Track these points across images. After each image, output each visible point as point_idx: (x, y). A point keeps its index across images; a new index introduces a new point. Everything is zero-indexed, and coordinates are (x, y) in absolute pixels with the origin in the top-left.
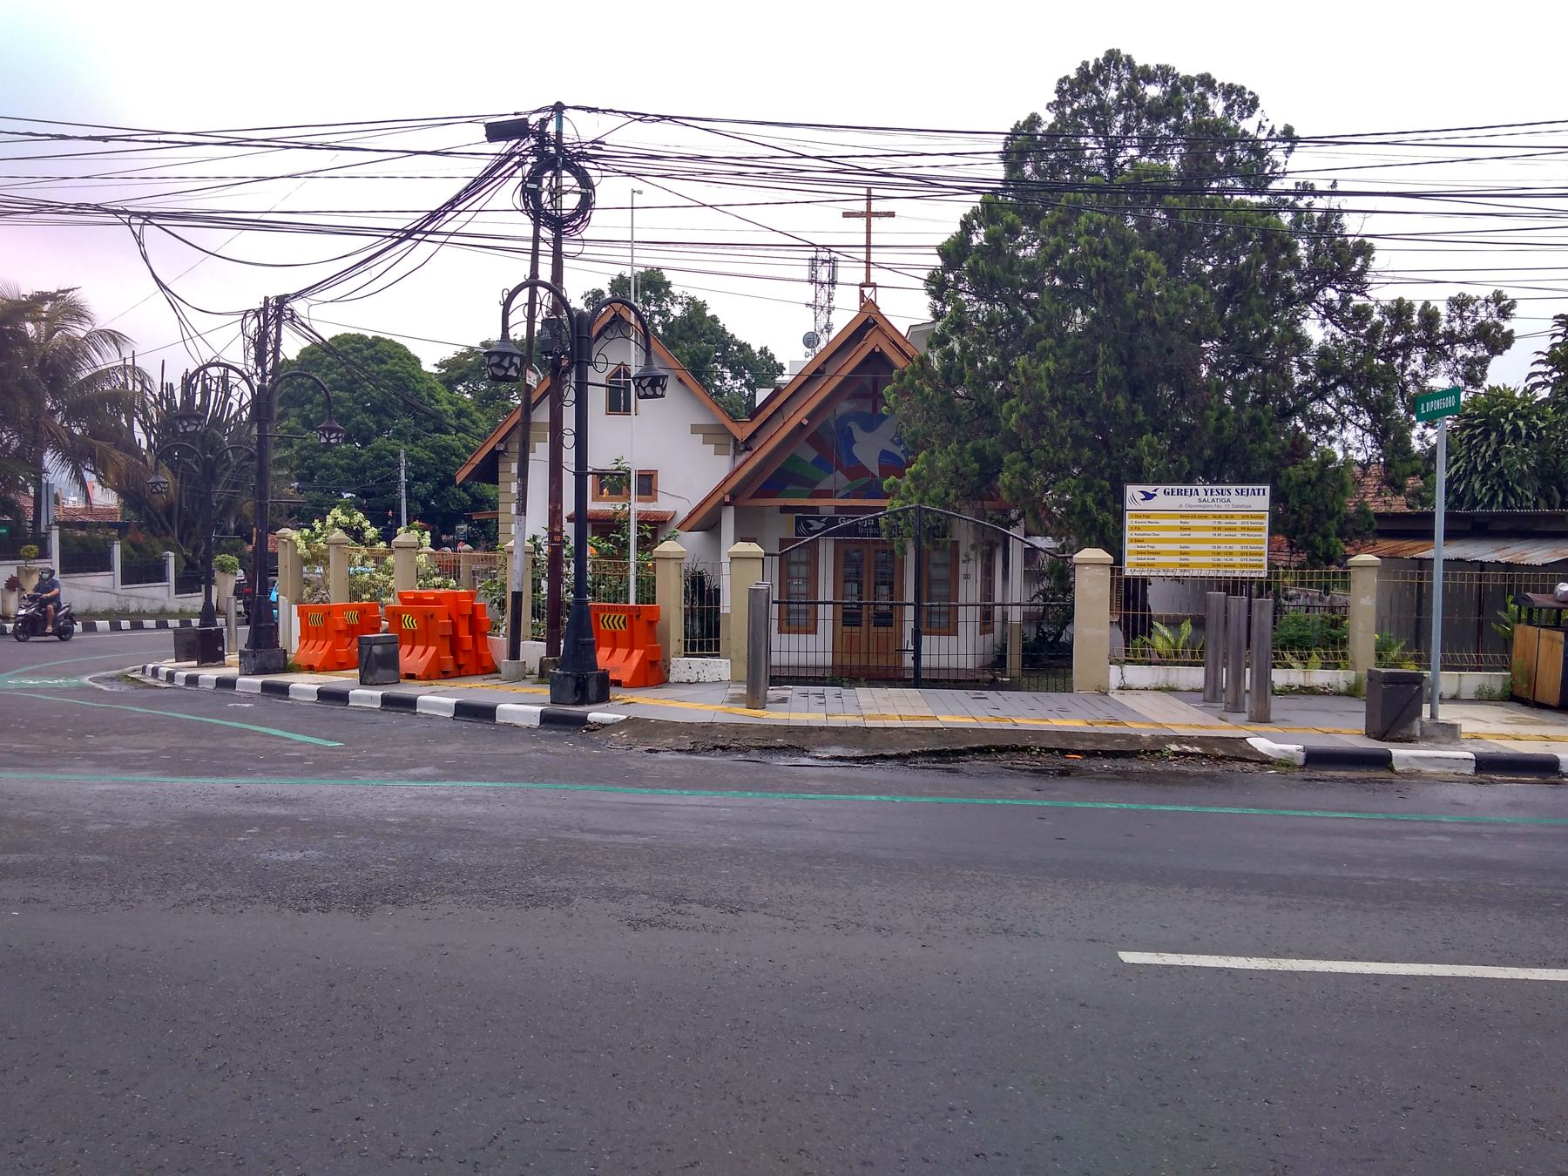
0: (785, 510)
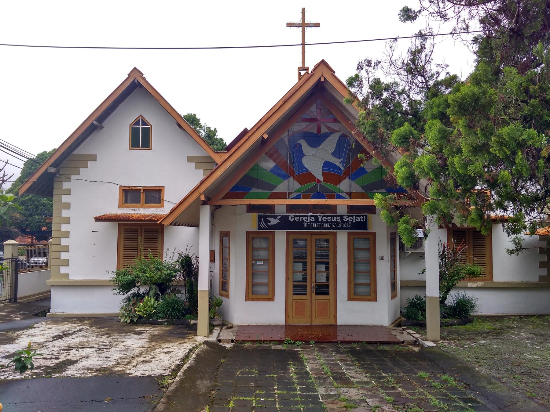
0: (251, 209)
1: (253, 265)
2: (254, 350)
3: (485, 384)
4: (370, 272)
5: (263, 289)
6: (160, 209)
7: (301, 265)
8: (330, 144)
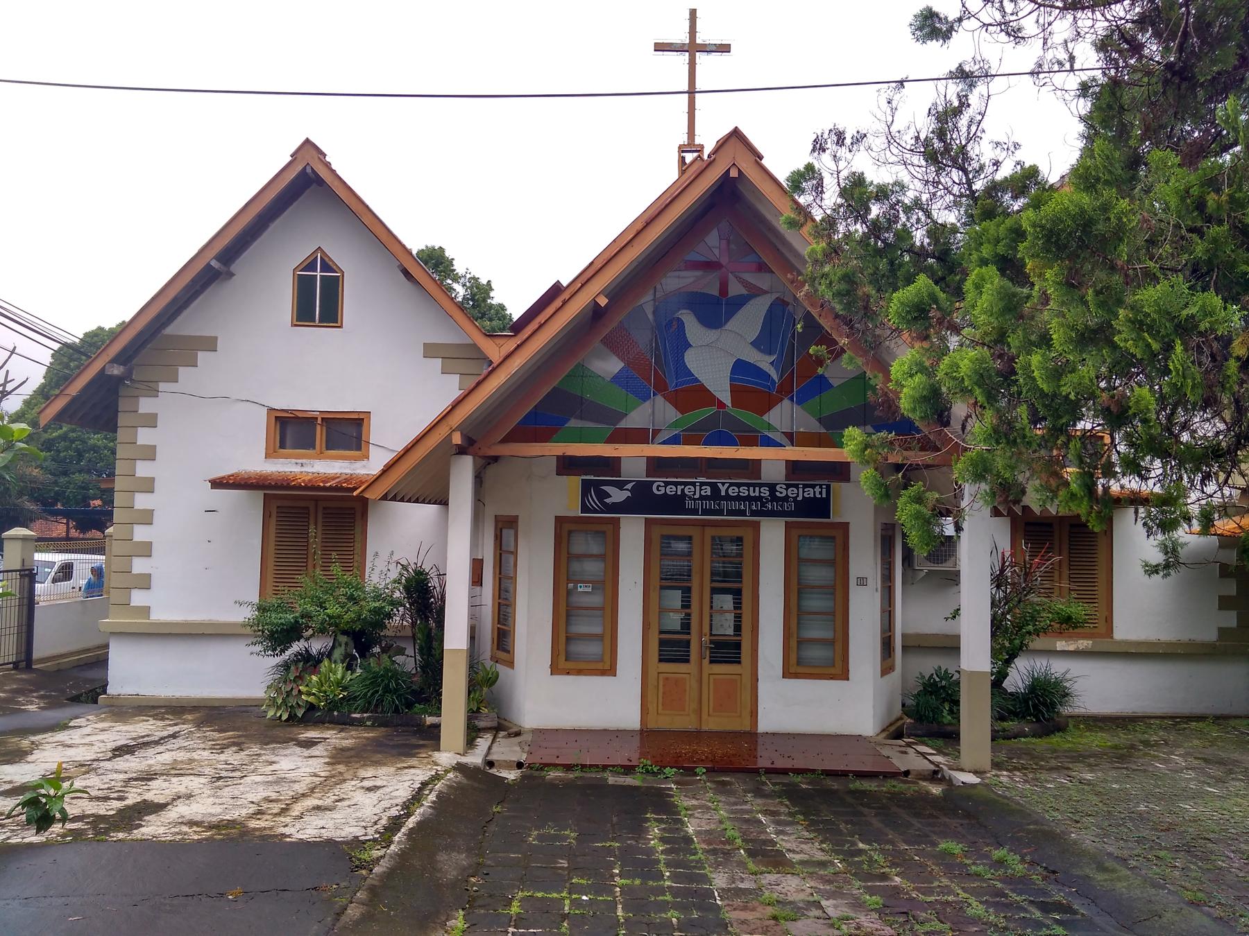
0: (567, 465)
1: (569, 593)
2: (569, 785)
3: (1089, 871)
4: (833, 614)
5: (593, 649)
6: (359, 464)
7: (678, 594)
8: (748, 322)
